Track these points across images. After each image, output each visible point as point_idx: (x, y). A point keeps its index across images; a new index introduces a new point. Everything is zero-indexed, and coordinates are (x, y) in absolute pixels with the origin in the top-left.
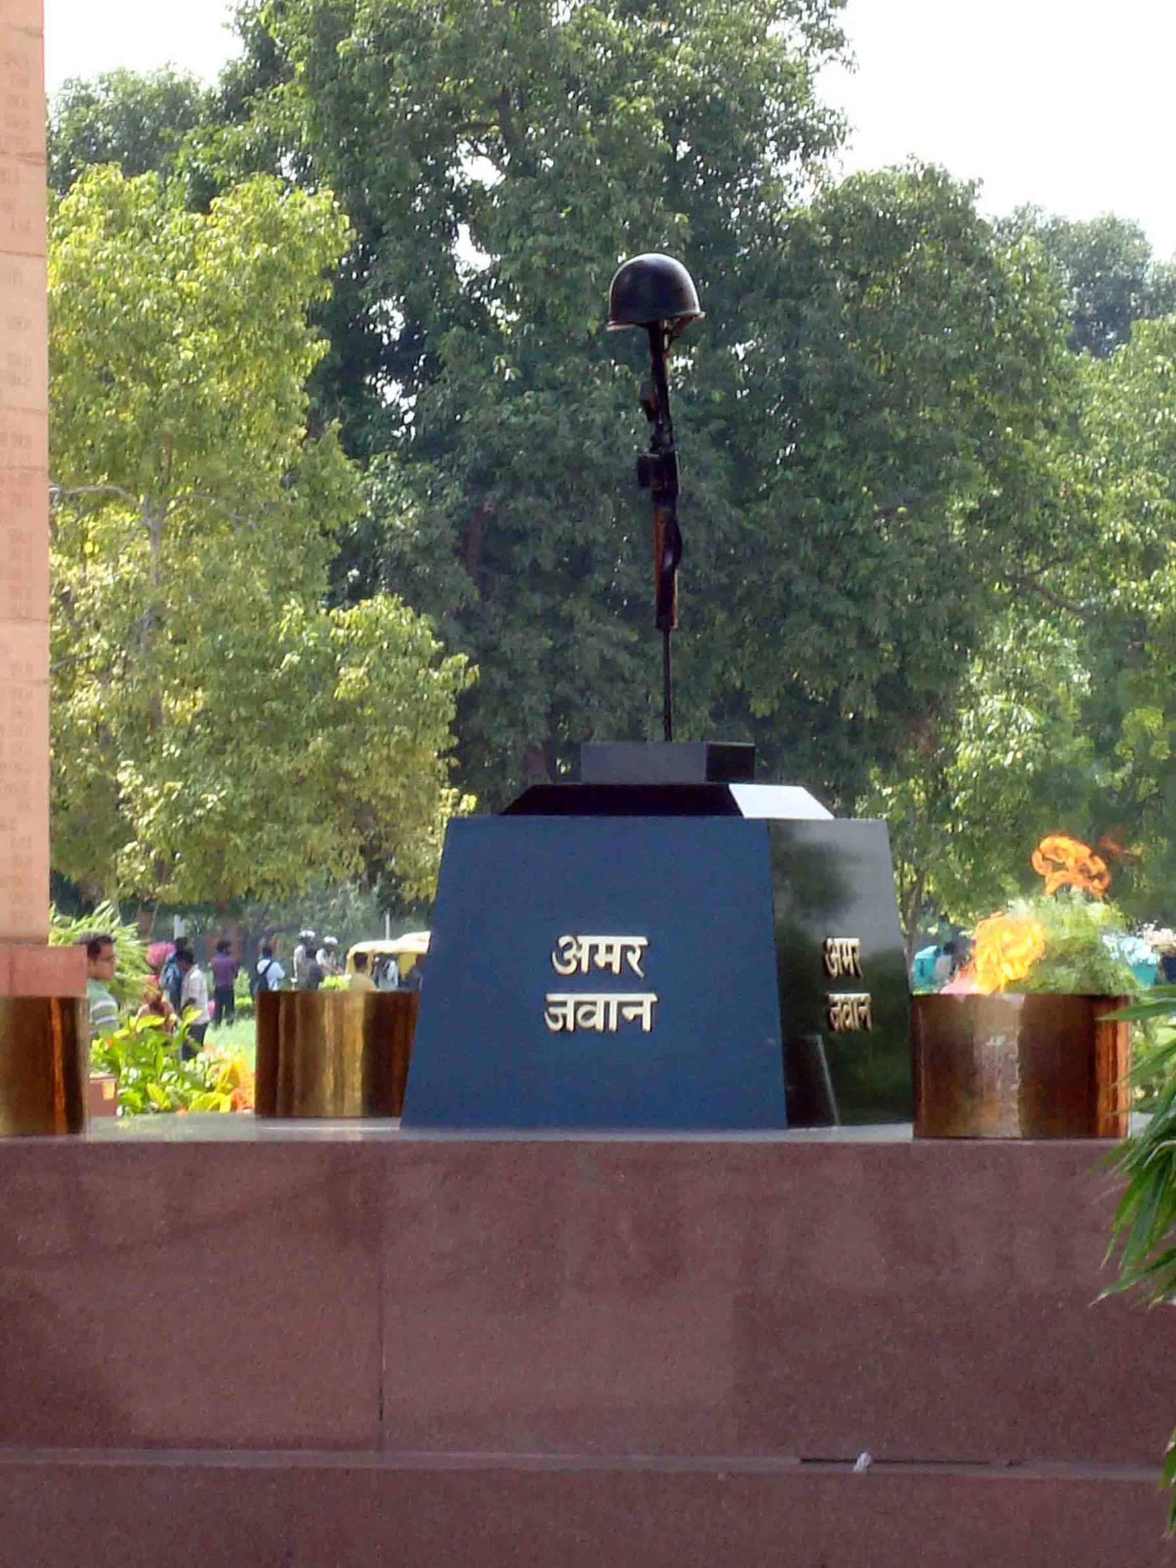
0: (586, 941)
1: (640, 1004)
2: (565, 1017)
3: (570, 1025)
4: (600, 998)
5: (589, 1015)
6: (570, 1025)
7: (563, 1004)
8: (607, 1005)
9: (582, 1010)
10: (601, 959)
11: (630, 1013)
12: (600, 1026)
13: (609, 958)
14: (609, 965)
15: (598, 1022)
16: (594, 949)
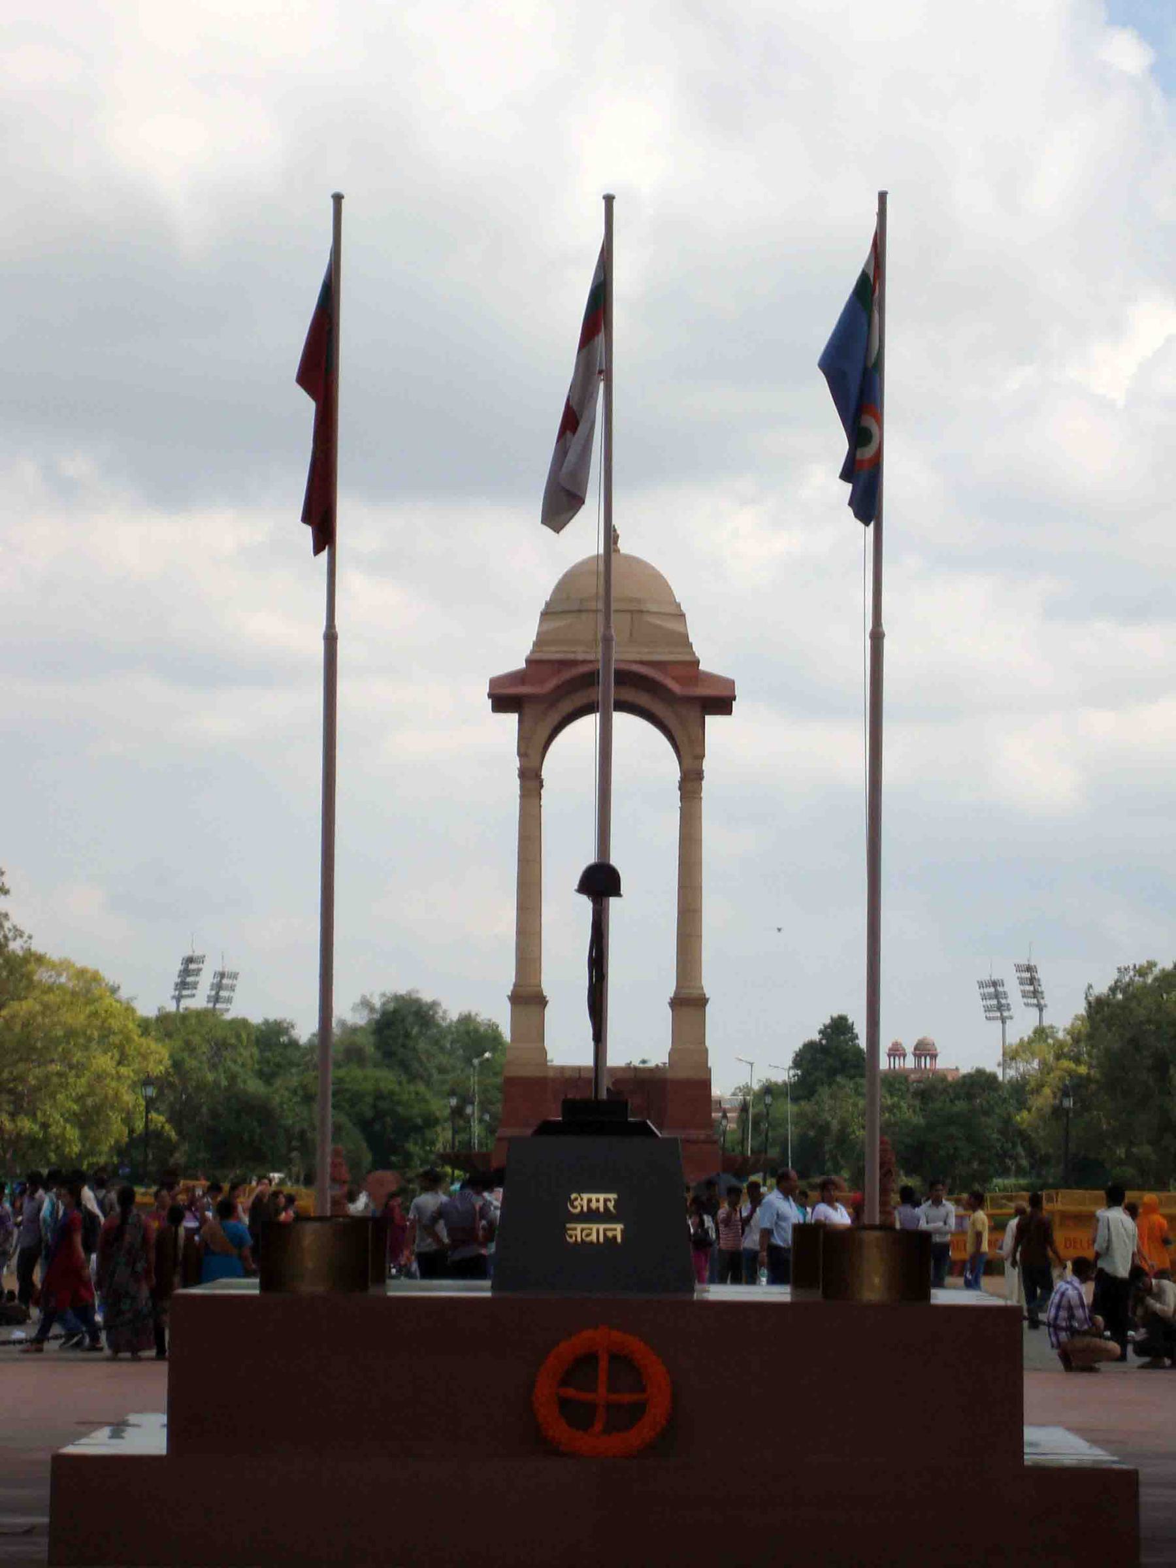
0: (585, 1196)
3: (579, 1239)
4: (594, 1227)
5: (588, 1235)
6: (579, 1239)
10: (594, 1205)
11: (610, 1234)
12: (595, 1239)
15: (594, 1237)
16: (590, 1201)
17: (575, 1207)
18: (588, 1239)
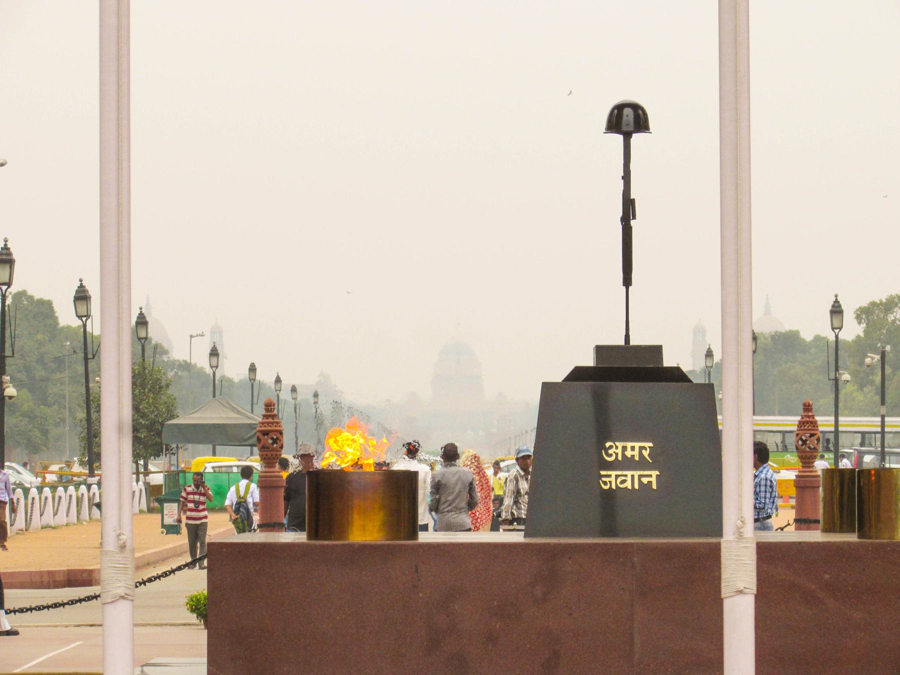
0: (620, 445)
1: (651, 476)
2: (610, 482)
3: (614, 487)
4: (629, 473)
5: (623, 482)
6: (614, 487)
7: (609, 476)
8: (633, 476)
9: (619, 480)
10: (629, 453)
11: (645, 480)
12: (630, 487)
13: (633, 453)
14: (633, 456)
15: (628, 485)
16: (624, 449)
17: (611, 455)
18: (621, 486)
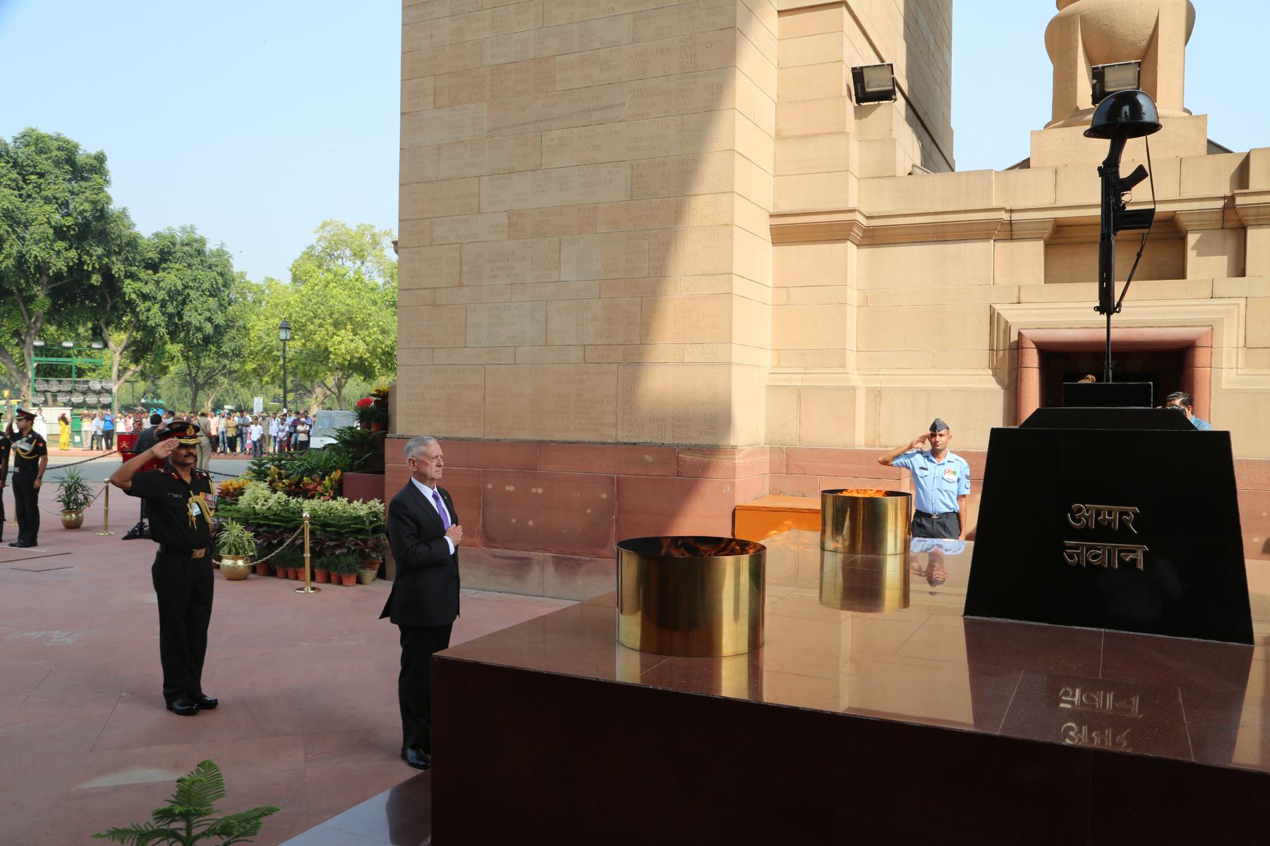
14: (1110, 522)
16: (1098, 513)
